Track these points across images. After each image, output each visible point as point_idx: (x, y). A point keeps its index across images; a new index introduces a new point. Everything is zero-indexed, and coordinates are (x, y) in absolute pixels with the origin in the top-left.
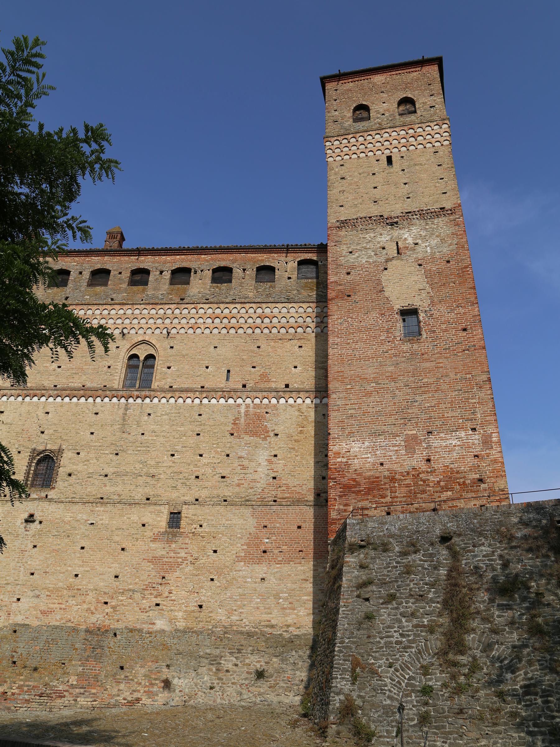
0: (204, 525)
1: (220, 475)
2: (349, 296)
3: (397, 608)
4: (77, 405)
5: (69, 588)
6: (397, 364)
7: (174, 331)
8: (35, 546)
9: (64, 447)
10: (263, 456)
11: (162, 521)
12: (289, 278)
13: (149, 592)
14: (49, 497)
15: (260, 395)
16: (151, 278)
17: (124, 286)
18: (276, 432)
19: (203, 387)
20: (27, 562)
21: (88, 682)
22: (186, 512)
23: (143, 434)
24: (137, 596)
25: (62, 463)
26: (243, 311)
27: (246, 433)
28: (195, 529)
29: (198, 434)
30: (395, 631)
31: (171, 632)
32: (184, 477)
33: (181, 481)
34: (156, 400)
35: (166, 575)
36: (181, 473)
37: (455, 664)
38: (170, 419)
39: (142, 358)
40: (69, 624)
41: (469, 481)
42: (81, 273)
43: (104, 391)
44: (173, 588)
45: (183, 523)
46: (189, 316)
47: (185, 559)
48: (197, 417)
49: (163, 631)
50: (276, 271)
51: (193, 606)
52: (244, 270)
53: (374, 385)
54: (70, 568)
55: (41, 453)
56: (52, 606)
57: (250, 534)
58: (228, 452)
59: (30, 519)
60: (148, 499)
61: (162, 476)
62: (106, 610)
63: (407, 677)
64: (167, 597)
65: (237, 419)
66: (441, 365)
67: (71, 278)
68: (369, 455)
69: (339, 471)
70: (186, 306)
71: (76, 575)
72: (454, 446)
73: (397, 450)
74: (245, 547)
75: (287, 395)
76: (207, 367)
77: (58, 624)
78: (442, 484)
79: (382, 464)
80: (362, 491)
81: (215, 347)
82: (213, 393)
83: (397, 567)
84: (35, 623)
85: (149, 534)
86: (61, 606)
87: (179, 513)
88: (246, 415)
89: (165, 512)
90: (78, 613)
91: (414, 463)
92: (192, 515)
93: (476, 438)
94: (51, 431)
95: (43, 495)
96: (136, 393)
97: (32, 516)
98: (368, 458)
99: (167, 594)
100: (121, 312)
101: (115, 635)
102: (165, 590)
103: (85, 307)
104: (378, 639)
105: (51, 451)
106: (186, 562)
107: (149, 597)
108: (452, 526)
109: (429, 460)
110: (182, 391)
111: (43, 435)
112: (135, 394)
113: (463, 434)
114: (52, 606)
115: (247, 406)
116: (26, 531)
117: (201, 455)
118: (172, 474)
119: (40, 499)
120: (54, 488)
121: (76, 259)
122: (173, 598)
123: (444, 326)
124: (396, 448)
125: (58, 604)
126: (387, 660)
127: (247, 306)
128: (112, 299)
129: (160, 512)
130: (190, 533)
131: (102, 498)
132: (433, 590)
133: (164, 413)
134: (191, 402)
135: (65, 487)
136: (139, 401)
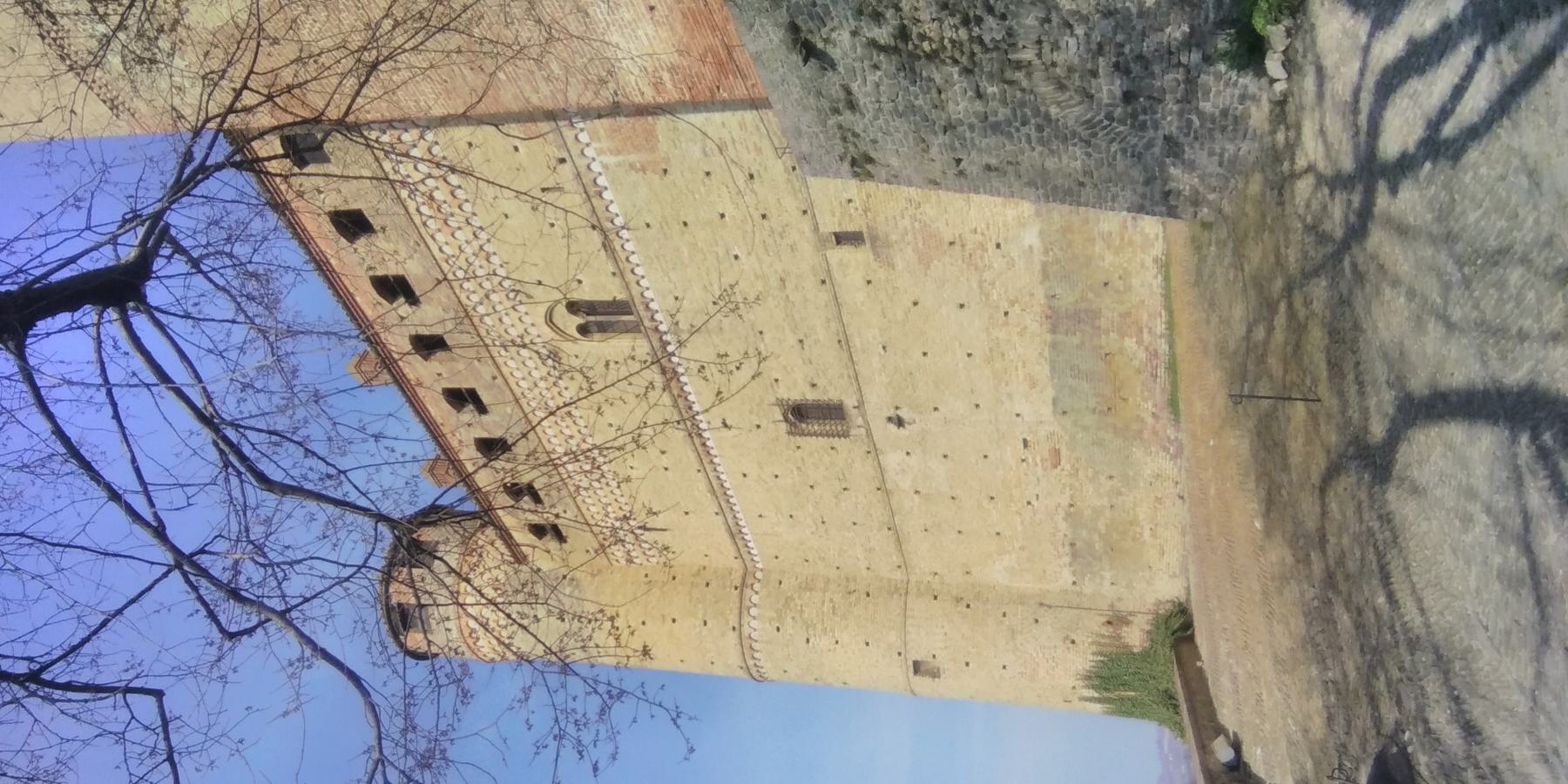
0: (846, 196)
4: (698, 394)
9: (773, 400)
21: (1128, 323)
22: (830, 225)
24: (987, 275)
25: (798, 398)
33: (778, 239)
34: (648, 294)
40: (1046, 353)
45: (851, 228)
47: (914, 218)
49: (1041, 233)
55: (792, 424)
58: (702, 175)
77: (1047, 368)
84: (1050, 393)
85: (881, 274)
88: (619, 153)
89: (838, 254)
90: (1028, 346)
96: (647, 323)
97: (890, 419)
102: (971, 241)
115: (600, 152)
117: (723, 216)
119: (864, 416)
129: (841, 263)
132: (924, 74)
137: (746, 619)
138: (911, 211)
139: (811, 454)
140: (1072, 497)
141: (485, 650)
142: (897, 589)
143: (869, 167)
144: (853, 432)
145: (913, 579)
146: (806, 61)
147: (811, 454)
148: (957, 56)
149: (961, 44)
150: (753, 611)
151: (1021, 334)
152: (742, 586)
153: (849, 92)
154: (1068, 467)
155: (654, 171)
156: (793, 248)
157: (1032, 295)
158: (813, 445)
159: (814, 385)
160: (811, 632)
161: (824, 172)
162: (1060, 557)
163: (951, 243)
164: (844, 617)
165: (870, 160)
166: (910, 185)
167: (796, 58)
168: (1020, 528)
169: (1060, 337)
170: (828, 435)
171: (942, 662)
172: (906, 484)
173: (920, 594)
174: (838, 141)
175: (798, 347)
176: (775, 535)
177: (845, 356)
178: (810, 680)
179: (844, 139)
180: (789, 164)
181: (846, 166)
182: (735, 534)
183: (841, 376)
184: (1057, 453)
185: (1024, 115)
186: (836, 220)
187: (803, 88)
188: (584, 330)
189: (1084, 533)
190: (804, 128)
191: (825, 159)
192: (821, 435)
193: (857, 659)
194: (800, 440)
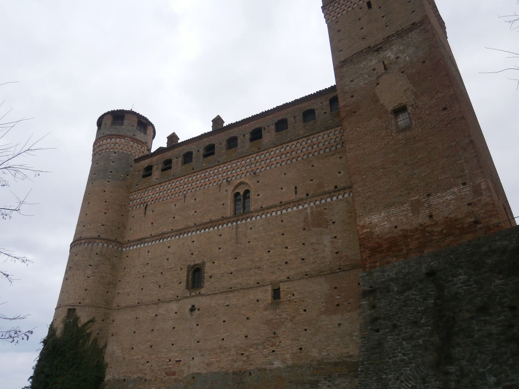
1: (301, 259)
2: (355, 112)
3: (398, 335)
4: (209, 232)
5: (220, 347)
6: (397, 150)
7: (258, 171)
8: (198, 325)
9: (205, 260)
10: (326, 240)
11: (269, 296)
12: (325, 113)
15: (318, 198)
16: (239, 141)
17: (224, 151)
18: (333, 221)
19: (281, 202)
22: (283, 287)
23: (249, 242)
24: (260, 347)
25: (205, 270)
26: (299, 145)
29: (283, 234)
30: (399, 352)
31: (285, 369)
33: (276, 268)
34: (254, 219)
35: (276, 331)
37: (447, 373)
39: (242, 193)
40: (223, 370)
41: (467, 225)
42: (198, 151)
43: (224, 220)
45: (282, 295)
46: (265, 158)
47: (286, 318)
48: (280, 223)
49: (279, 368)
50: (316, 111)
51: (296, 350)
52: (294, 117)
53: (382, 170)
56: (212, 360)
57: (326, 294)
58: (303, 242)
59: (193, 309)
60: (258, 283)
61: (265, 267)
62: (243, 359)
63: (410, 386)
64: (279, 345)
65: (306, 218)
66: (430, 141)
67: (194, 156)
68: (386, 223)
69: (366, 239)
70: (262, 153)
71: (223, 339)
72: (450, 200)
73: (406, 214)
74: (324, 304)
75: (337, 194)
76: (282, 189)
77: (216, 370)
78: (444, 231)
79: (396, 227)
80: (385, 250)
81: (285, 174)
82: (288, 205)
83: (396, 303)
84: (204, 372)
85: (262, 306)
87: (279, 289)
89: (269, 288)
91: (421, 221)
93: (467, 190)
94: (197, 252)
95: (198, 292)
97: (193, 306)
98: (385, 225)
99: (278, 344)
100: (225, 168)
101: (250, 374)
103: (204, 171)
104: (387, 359)
105: (198, 264)
108: (434, 264)
109: (431, 216)
110: (268, 208)
111: (193, 256)
113: (456, 189)
114: (212, 360)
115: (312, 208)
117: (287, 248)
119: (196, 295)
120: (203, 287)
121: (195, 143)
122: (282, 345)
123: (428, 112)
124: (405, 213)
126: (395, 374)
127: (300, 141)
128: (218, 162)
131: (231, 288)
132: (424, 316)
136: (244, 221)
137: (104, 242)
140: (150, 380)
141: (101, 142)
147: (178, 274)
150: (106, 245)
154: (166, 379)
156: (273, 273)
159: (211, 277)
162: (119, 375)
163: (275, 333)
168: (135, 357)
172: (161, 311)
180: (308, 273)
183: (215, 288)
184: (174, 374)
186: (285, 289)
188: (238, 194)
189: (131, 385)
194: (185, 270)
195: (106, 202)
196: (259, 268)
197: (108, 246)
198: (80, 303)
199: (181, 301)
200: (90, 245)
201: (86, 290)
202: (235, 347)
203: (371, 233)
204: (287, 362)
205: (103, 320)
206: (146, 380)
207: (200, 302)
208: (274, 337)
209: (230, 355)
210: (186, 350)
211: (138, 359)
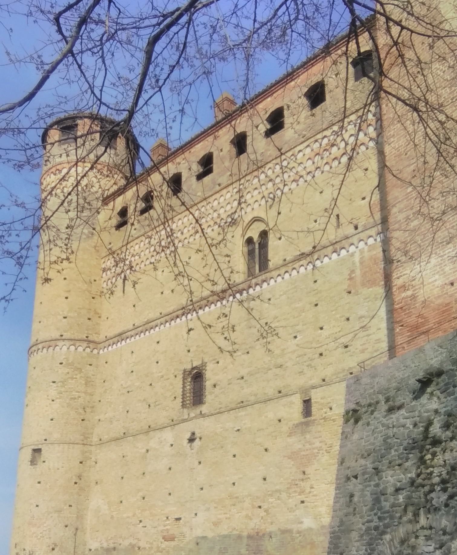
4: (210, 313)
9: (206, 360)
13: (293, 490)
14: (203, 413)
20: (196, 479)
22: (316, 396)
25: (207, 376)
27: (363, 285)
28: (326, 413)
32: (309, 358)
34: (272, 282)
36: (305, 355)
38: (288, 298)
40: (235, 532)
44: (313, 482)
45: (314, 409)
47: (320, 449)
49: (311, 529)
54: (228, 478)
55: (190, 372)
60: (280, 392)
62: (261, 515)
64: (310, 492)
71: (234, 484)
77: (225, 533)
84: (210, 535)
86: (226, 515)
89: (297, 401)
92: (321, 399)
96: (254, 281)
97: (193, 434)
102: (306, 485)
106: (321, 452)
107: (294, 495)
111: (190, 354)
112: (254, 283)
114: (219, 517)
116: (192, 449)
117: (321, 328)
118: (298, 359)
119: (195, 417)
120: (205, 403)
122: (315, 493)
125: (224, 514)
129: (292, 403)
130: (321, 419)
133: (282, 293)
134: (305, 271)
135: (213, 400)
138: (325, 447)
139: (171, 384)
140: (145, 548)
142: (86, 438)
143: (352, 421)
144: (185, 410)
145: (93, 448)
146: (419, 381)
147: (171, 384)
148: (422, 476)
149: (429, 479)
151: (247, 516)
152: (89, 341)
153: (399, 408)
154: (163, 546)
155: (349, 286)
156: (301, 373)
157: (272, 523)
158: (177, 386)
159: (215, 386)
160: (59, 384)
161: (349, 392)
162: (107, 541)
163: (304, 473)
164: (69, 405)
165: (356, 421)
166: (341, 447)
167: (421, 375)
168: (125, 515)
169: (245, 541)
170: (184, 395)
171: (41, 467)
172: (153, 444)
173: (83, 452)
174: (368, 401)
175: (239, 376)
176: (120, 360)
177: (233, 406)
178: (29, 383)
179: (370, 405)
180: (354, 371)
181: (353, 406)
182: (121, 336)
183: (220, 403)
184: (172, 539)
185: (385, 519)
186: (319, 400)
187: (402, 379)
190: (377, 380)
191: (357, 393)
192: (184, 391)
193: (43, 412)
195: (65, 279)
196: (281, 366)
197: (76, 349)
198: (46, 440)
199: (176, 427)
200: (51, 349)
201: (52, 420)
202: (250, 495)
203: (414, 297)
204: (322, 519)
205: (81, 463)
206: (139, 548)
207: (203, 426)
208: (303, 480)
209: (243, 509)
210: (186, 502)
211: (128, 517)
